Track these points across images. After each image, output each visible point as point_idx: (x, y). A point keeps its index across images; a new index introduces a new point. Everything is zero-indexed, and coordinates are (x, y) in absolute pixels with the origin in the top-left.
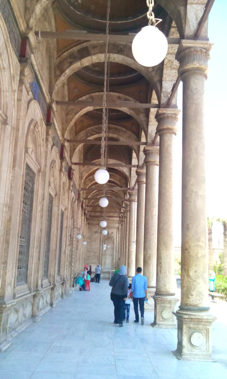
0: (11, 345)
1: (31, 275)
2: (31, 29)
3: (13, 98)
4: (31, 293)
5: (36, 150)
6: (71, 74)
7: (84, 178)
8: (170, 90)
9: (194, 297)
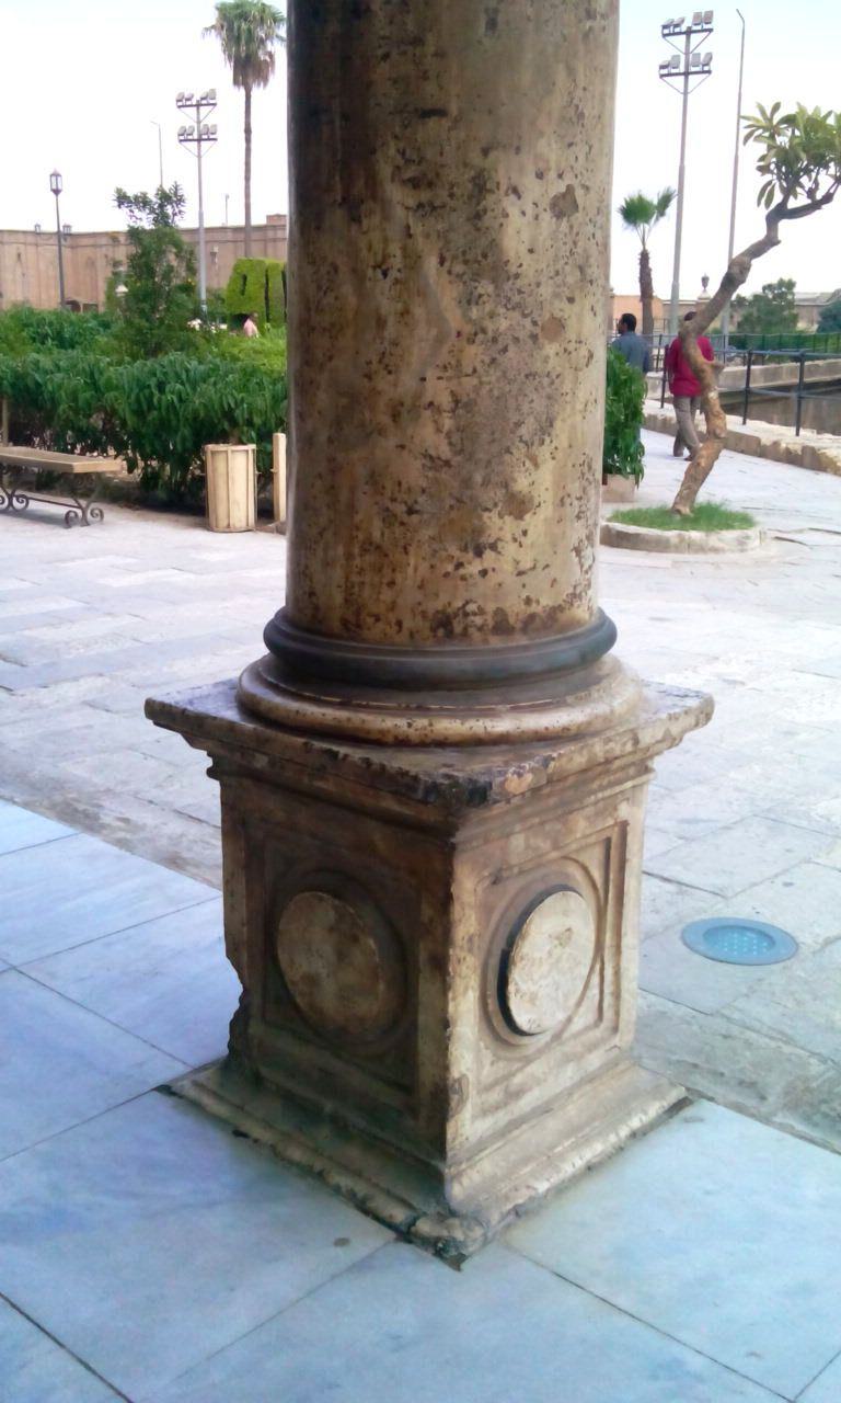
9: (535, 523)
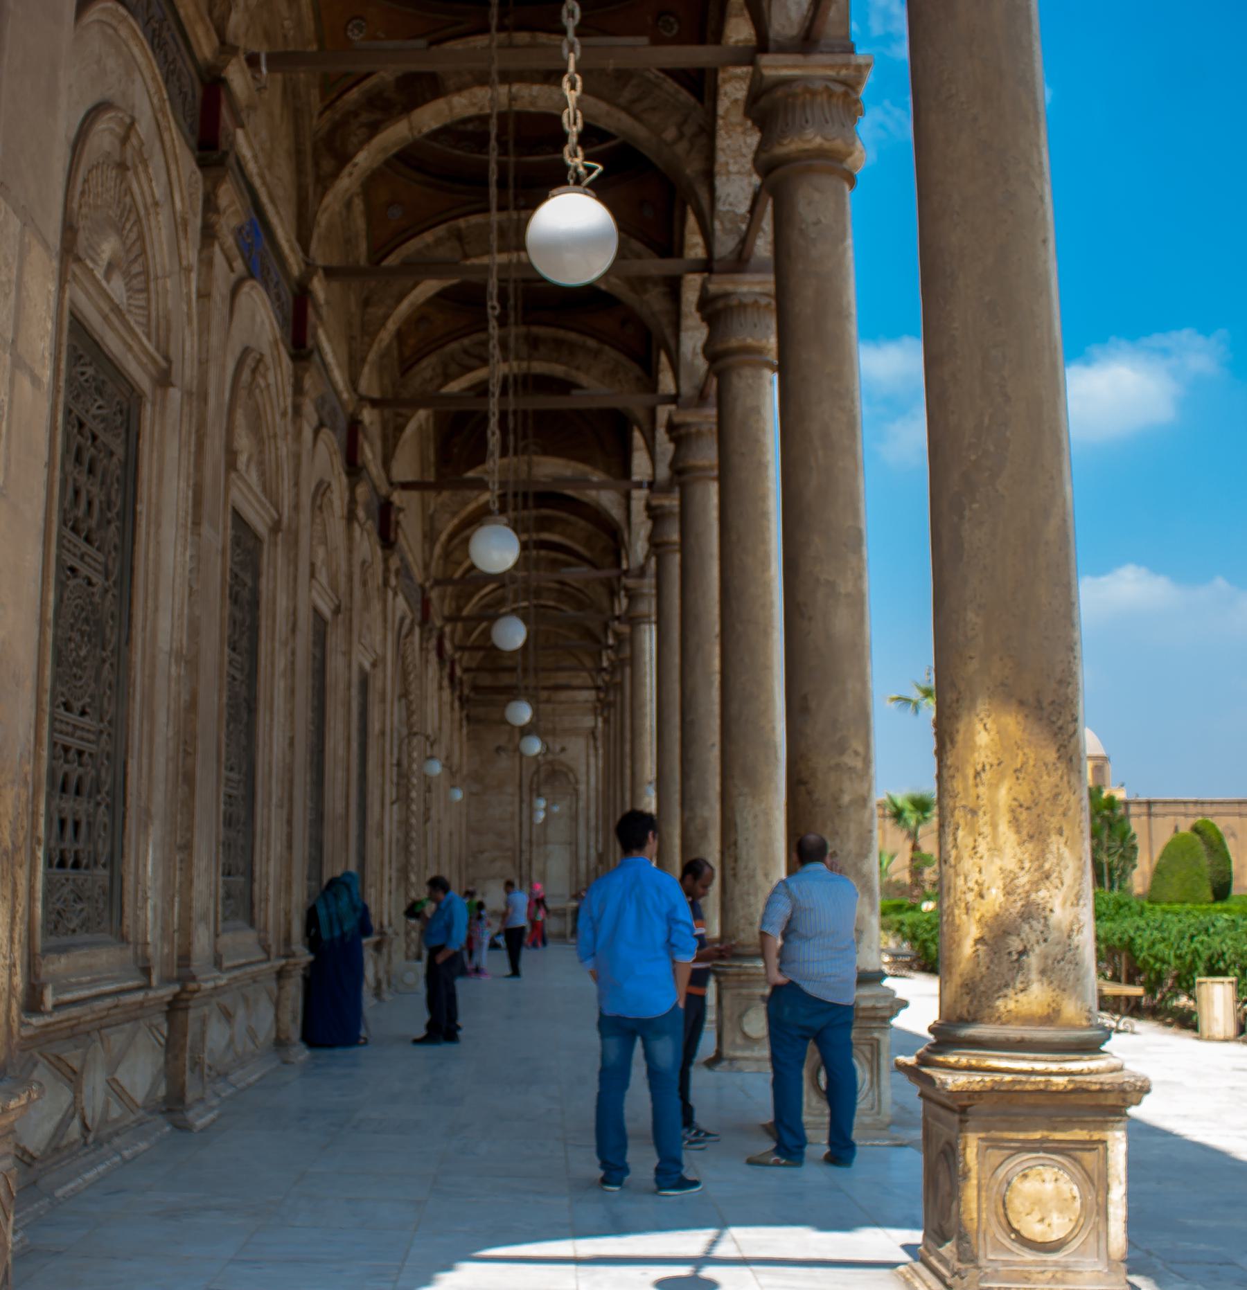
0: (220, 1116)
1: (267, 900)
2: (234, 50)
3: (185, 291)
4: (268, 959)
5: (261, 452)
6: (375, 166)
7: (443, 537)
8: (743, 209)
